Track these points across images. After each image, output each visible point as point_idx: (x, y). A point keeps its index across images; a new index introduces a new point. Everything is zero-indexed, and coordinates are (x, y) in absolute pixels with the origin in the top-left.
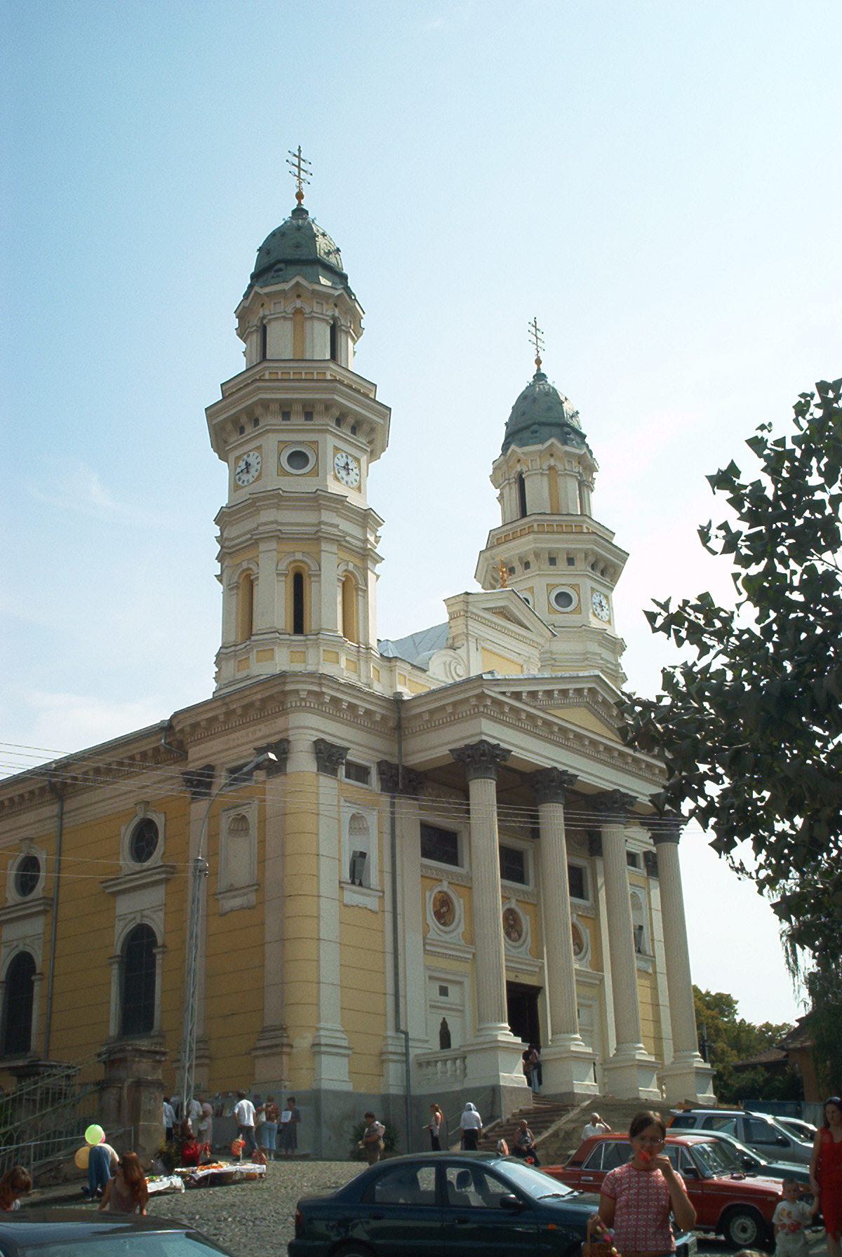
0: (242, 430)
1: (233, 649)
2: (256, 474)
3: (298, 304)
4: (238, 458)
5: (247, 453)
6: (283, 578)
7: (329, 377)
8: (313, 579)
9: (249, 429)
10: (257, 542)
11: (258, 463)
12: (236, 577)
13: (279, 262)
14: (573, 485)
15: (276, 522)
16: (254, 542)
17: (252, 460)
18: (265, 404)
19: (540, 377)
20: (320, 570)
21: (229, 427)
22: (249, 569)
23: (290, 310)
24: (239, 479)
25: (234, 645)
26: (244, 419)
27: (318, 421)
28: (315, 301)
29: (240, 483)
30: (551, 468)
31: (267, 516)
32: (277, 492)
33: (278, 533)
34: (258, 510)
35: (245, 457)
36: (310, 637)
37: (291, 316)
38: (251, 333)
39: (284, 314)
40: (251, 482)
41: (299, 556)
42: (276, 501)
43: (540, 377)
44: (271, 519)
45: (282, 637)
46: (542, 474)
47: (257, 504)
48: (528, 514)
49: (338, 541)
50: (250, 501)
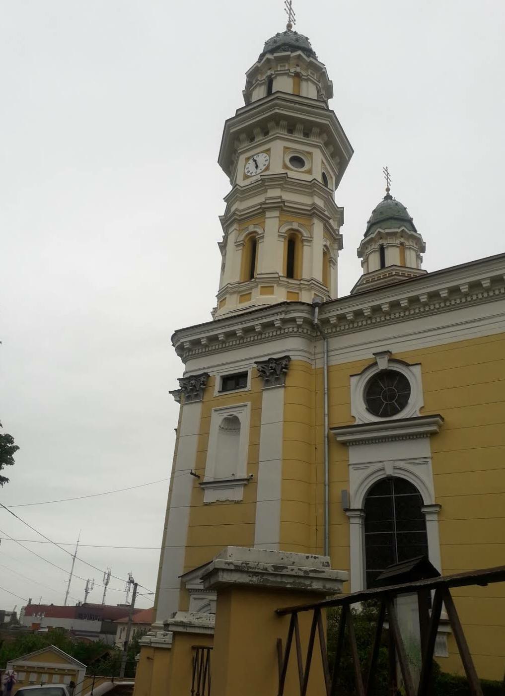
0: (252, 139)
2: (264, 168)
3: (298, 69)
4: (248, 159)
6: (283, 240)
8: (305, 243)
9: (259, 139)
10: (264, 212)
12: (244, 236)
14: (413, 254)
16: (261, 211)
18: (277, 119)
19: (388, 197)
20: (311, 237)
21: (243, 136)
22: (255, 232)
23: (292, 70)
24: (248, 172)
27: (313, 140)
29: (249, 174)
30: (402, 244)
32: (284, 175)
34: (265, 191)
36: (302, 282)
37: (293, 75)
38: (260, 85)
41: (295, 226)
43: (388, 197)
45: (281, 279)
46: (397, 247)
48: (386, 266)
49: (325, 220)
50: (261, 182)
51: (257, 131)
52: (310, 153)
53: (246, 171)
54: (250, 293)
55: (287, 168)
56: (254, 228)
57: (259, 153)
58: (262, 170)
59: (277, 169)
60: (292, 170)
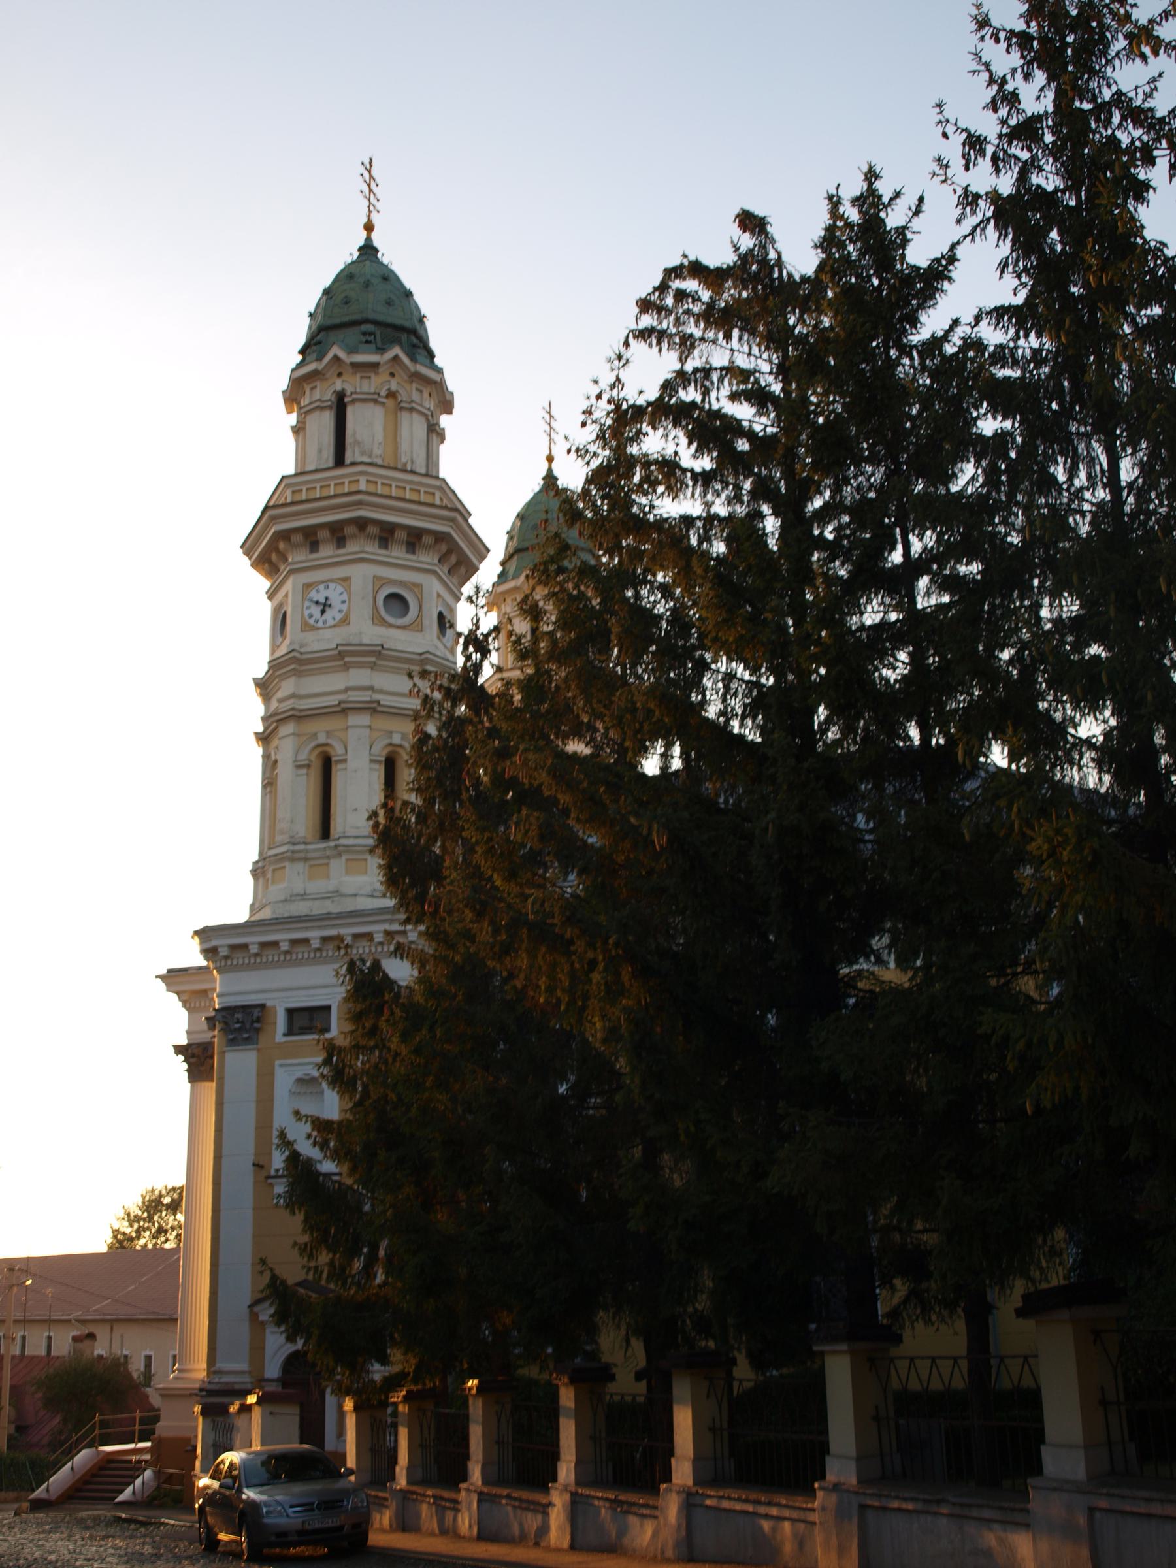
1: (302, 847)
2: (339, 617)
4: (308, 586)
5: (326, 582)
7: (438, 502)
11: (343, 602)
13: (366, 321)
15: (371, 688)
17: (335, 594)
18: (362, 524)
22: (327, 745)
24: (311, 616)
25: (305, 843)
26: (323, 534)
28: (414, 385)
29: (312, 621)
31: (359, 677)
33: (375, 705)
35: (321, 587)
39: (376, 397)
40: (330, 622)
42: (373, 659)
44: (366, 682)
47: (347, 659)
51: (323, 534)
52: (420, 586)
53: (306, 613)
54: (327, 864)
55: (384, 623)
56: (328, 737)
57: (332, 581)
58: (338, 619)
59: (366, 631)
60: (391, 626)
